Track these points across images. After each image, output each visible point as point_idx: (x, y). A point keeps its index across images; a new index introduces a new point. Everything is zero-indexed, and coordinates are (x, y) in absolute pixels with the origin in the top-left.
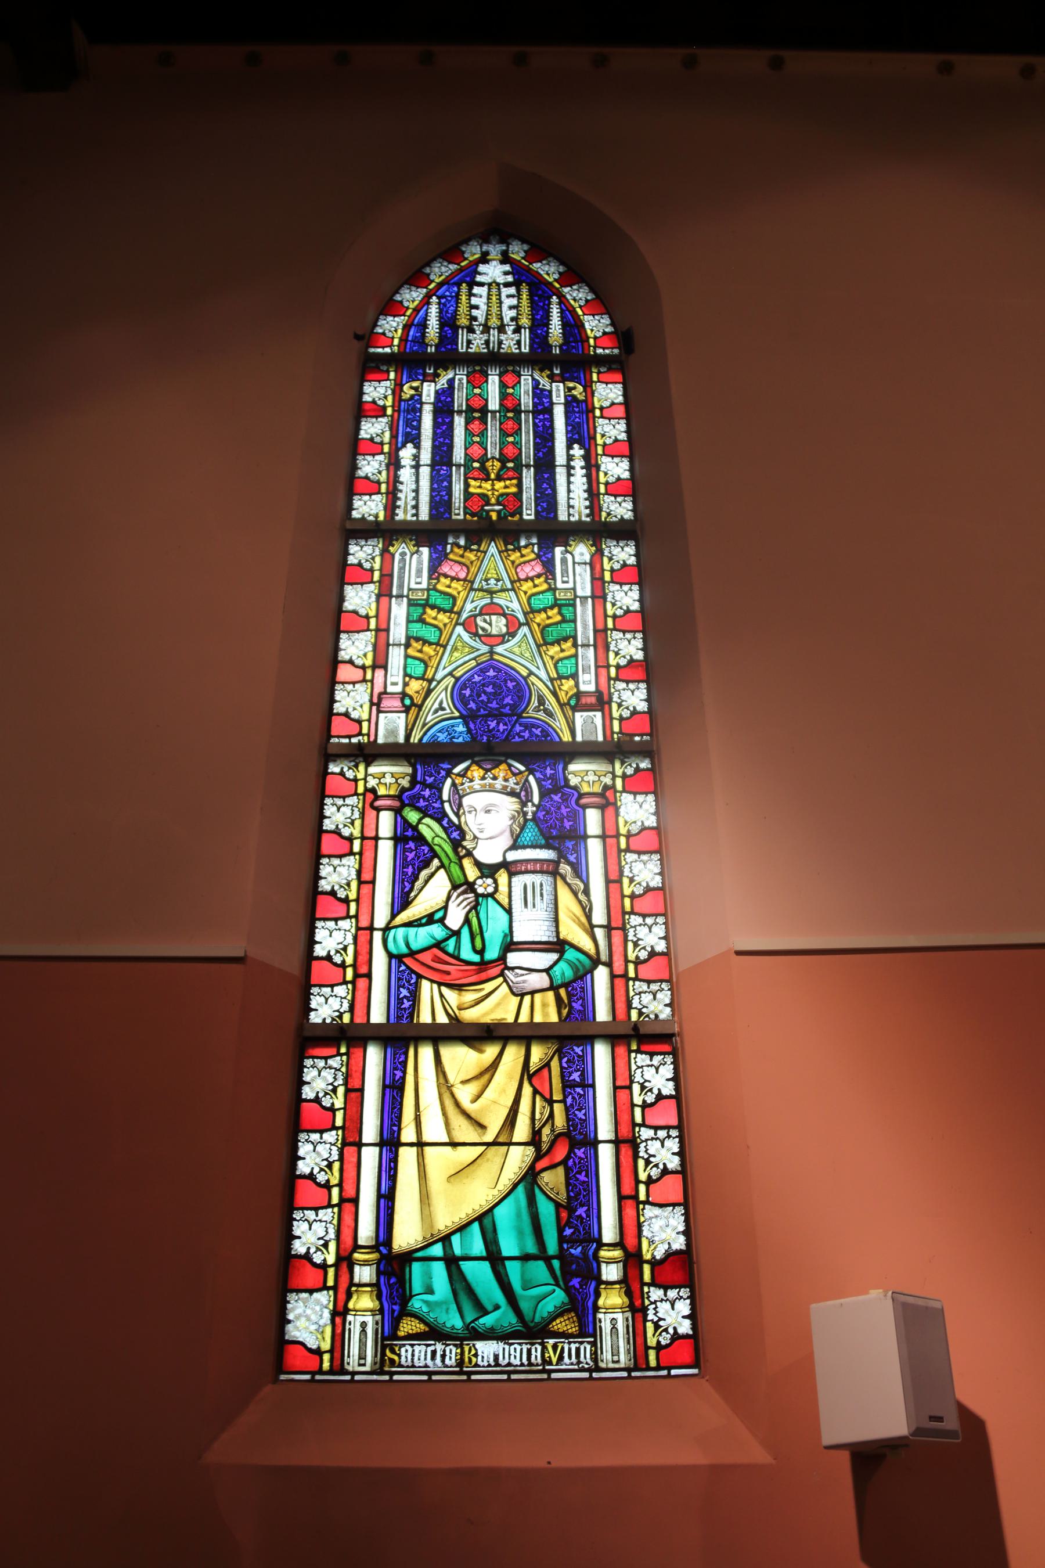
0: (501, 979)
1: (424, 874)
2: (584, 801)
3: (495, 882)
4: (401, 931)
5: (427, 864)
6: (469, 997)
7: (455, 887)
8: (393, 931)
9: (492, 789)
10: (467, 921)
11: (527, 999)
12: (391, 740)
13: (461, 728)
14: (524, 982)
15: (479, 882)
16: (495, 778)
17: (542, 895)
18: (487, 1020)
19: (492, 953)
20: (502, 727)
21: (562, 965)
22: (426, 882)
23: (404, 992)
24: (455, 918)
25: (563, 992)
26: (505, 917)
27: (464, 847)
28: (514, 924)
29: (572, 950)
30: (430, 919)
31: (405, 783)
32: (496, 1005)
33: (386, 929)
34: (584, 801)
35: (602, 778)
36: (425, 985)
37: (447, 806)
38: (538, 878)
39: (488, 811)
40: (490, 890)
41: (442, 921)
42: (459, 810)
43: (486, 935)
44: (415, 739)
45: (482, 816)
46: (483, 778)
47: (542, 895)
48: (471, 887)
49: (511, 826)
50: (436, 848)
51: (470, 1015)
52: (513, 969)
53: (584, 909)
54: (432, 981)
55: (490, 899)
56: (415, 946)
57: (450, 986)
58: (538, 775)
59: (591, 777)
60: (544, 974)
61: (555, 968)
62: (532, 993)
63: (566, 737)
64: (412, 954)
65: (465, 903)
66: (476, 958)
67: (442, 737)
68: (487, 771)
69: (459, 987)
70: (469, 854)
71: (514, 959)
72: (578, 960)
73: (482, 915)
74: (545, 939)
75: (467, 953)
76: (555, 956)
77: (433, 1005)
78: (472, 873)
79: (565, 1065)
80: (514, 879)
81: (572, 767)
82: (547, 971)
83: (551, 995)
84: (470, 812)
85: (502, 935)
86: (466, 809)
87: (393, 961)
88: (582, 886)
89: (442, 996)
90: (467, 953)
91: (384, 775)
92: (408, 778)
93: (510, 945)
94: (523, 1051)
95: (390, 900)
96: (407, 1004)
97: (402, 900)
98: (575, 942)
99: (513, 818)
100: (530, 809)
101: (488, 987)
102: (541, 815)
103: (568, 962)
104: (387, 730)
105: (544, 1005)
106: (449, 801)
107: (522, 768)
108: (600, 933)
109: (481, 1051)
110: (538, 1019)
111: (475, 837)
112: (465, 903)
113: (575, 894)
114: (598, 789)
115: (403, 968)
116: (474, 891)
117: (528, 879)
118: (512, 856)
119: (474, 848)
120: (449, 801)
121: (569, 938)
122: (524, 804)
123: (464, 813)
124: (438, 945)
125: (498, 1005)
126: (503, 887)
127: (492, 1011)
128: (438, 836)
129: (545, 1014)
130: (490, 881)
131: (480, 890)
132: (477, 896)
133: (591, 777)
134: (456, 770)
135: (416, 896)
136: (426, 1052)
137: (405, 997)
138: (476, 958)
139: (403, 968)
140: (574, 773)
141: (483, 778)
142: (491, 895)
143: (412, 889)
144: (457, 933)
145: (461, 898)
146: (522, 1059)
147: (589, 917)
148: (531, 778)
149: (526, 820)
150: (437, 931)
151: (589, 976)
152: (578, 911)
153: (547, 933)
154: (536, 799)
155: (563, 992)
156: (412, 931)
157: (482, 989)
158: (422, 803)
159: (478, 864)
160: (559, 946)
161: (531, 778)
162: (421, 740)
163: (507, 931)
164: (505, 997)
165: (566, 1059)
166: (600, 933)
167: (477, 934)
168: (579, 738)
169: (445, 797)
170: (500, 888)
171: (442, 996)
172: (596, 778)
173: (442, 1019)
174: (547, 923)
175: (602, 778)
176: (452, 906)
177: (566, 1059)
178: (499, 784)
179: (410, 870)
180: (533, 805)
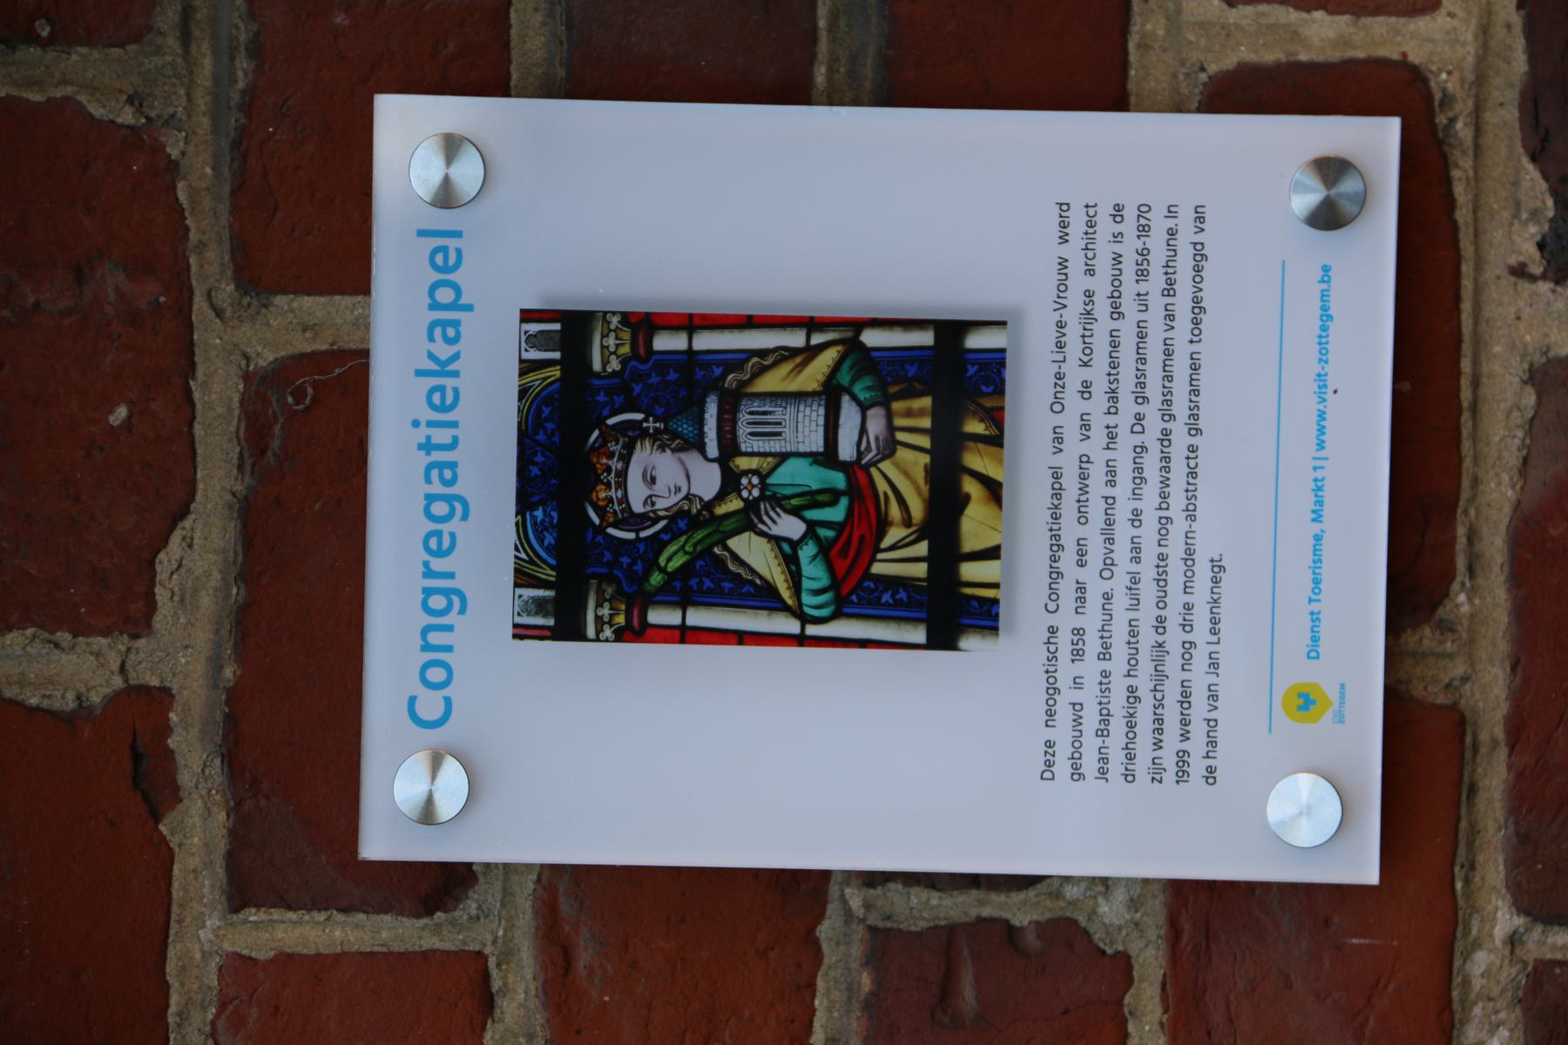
0: (873, 471)
1: (732, 567)
2: (642, 351)
3: (746, 473)
4: (807, 599)
5: (720, 562)
6: (895, 512)
7: (750, 527)
8: (807, 610)
9: (623, 475)
10: (796, 512)
11: (900, 436)
12: (550, 608)
13: (539, 514)
14: (877, 439)
15: (745, 494)
16: (608, 469)
17: (765, 413)
18: (925, 489)
19: (838, 480)
20: (539, 459)
21: (858, 389)
22: (742, 563)
23: (887, 597)
24: (790, 527)
25: (893, 389)
26: (791, 464)
27: (699, 512)
28: (802, 449)
29: (838, 376)
30: (791, 562)
31: (610, 590)
32: (905, 478)
33: (805, 620)
34: (642, 351)
35: (613, 327)
36: (877, 568)
37: (643, 534)
38: (744, 417)
39: (653, 480)
40: (755, 480)
41: (795, 545)
42: (650, 519)
43: (815, 486)
44: (549, 575)
45: (660, 488)
46: (608, 485)
47: (765, 413)
48: (751, 506)
49: (673, 451)
50: (699, 548)
51: (917, 510)
52: (860, 454)
53: (783, 359)
54: (873, 560)
55: (769, 481)
56: (825, 581)
57: (881, 534)
58: (606, 411)
59: (611, 341)
60: (870, 413)
61: (862, 396)
62: (891, 428)
63: (555, 372)
64: (835, 585)
65: (772, 514)
66: (844, 502)
67: (549, 539)
68: (598, 481)
69: (883, 525)
70: (709, 506)
71: (846, 451)
72: (851, 368)
73: (788, 491)
74: (822, 411)
75: (837, 513)
76: (846, 399)
77: (902, 559)
78: (734, 504)
79: (991, 389)
80: (743, 448)
81: (597, 366)
82: (864, 408)
83: (897, 406)
84: (653, 504)
85: (815, 468)
86: (649, 508)
87: (846, 610)
88: (755, 359)
89: (893, 548)
90: (837, 513)
91: (598, 619)
92: (604, 586)
93: (827, 457)
94: (971, 444)
95: (765, 612)
96: (902, 595)
97: (763, 596)
98: (826, 370)
99: (662, 448)
100: (651, 425)
101: (882, 486)
102: (659, 410)
103: (852, 382)
104: (537, 614)
105: (909, 413)
106: (637, 532)
107: (596, 433)
108: (817, 339)
109: (967, 499)
110: (926, 423)
111: (687, 498)
112: (772, 514)
113: (763, 370)
114: (626, 335)
115: (854, 598)
116: (757, 501)
117: (743, 430)
118: (713, 450)
119: (701, 499)
120: (637, 532)
121: (821, 378)
122: (644, 434)
123: (654, 512)
124: (825, 550)
125: (906, 474)
126: (753, 463)
127: (914, 483)
128: (682, 547)
129: (921, 413)
130: (744, 481)
131: (756, 493)
132: (762, 497)
133: (611, 341)
134: (596, 520)
135: (761, 578)
136: (970, 571)
137: (893, 596)
138: (844, 502)
139: (854, 598)
140: (605, 363)
141: (608, 485)
142: (763, 477)
143: (752, 583)
144: (812, 525)
145: (765, 518)
146: (980, 446)
147: (791, 353)
148: (610, 422)
149: (666, 431)
150: (807, 552)
151: (874, 354)
152: (786, 368)
153: (815, 407)
154: (639, 416)
155: (893, 389)
156: (806, 584)
157: (886, 494)
158: (639, 567)
159: (721, 496)
160: (830, 395)
161: (610, 422)
162: (552, 567)
163: (810, 460)
164: (897, 465)
165: (984, 388)
166: (817, 339)
167: (816, 498)
168: (557, 355)
169: (631, 536)
170: (754, 466)
171: (893, 548)
172: (612, 335)
173: (922, 548)
174: (802, 408)
175: (613, 327)
176: (776, 530)
177: (984, 388)
178: (616, 464)
179: (727, 585)
180: (646, 420)
